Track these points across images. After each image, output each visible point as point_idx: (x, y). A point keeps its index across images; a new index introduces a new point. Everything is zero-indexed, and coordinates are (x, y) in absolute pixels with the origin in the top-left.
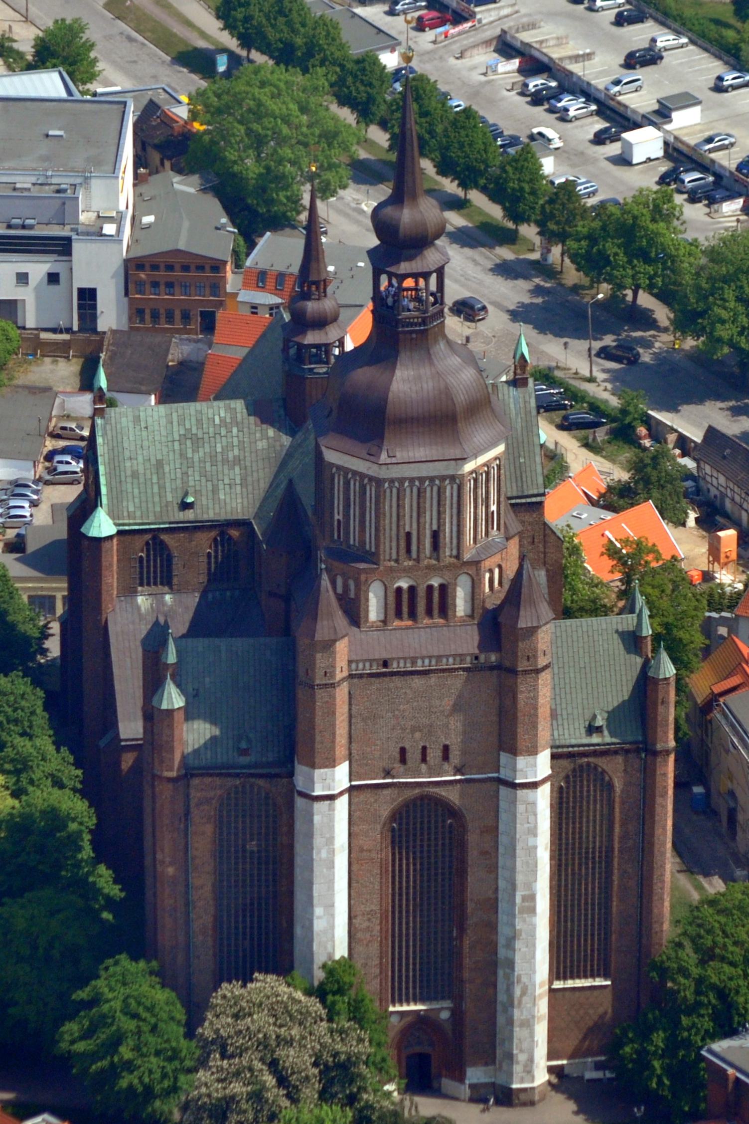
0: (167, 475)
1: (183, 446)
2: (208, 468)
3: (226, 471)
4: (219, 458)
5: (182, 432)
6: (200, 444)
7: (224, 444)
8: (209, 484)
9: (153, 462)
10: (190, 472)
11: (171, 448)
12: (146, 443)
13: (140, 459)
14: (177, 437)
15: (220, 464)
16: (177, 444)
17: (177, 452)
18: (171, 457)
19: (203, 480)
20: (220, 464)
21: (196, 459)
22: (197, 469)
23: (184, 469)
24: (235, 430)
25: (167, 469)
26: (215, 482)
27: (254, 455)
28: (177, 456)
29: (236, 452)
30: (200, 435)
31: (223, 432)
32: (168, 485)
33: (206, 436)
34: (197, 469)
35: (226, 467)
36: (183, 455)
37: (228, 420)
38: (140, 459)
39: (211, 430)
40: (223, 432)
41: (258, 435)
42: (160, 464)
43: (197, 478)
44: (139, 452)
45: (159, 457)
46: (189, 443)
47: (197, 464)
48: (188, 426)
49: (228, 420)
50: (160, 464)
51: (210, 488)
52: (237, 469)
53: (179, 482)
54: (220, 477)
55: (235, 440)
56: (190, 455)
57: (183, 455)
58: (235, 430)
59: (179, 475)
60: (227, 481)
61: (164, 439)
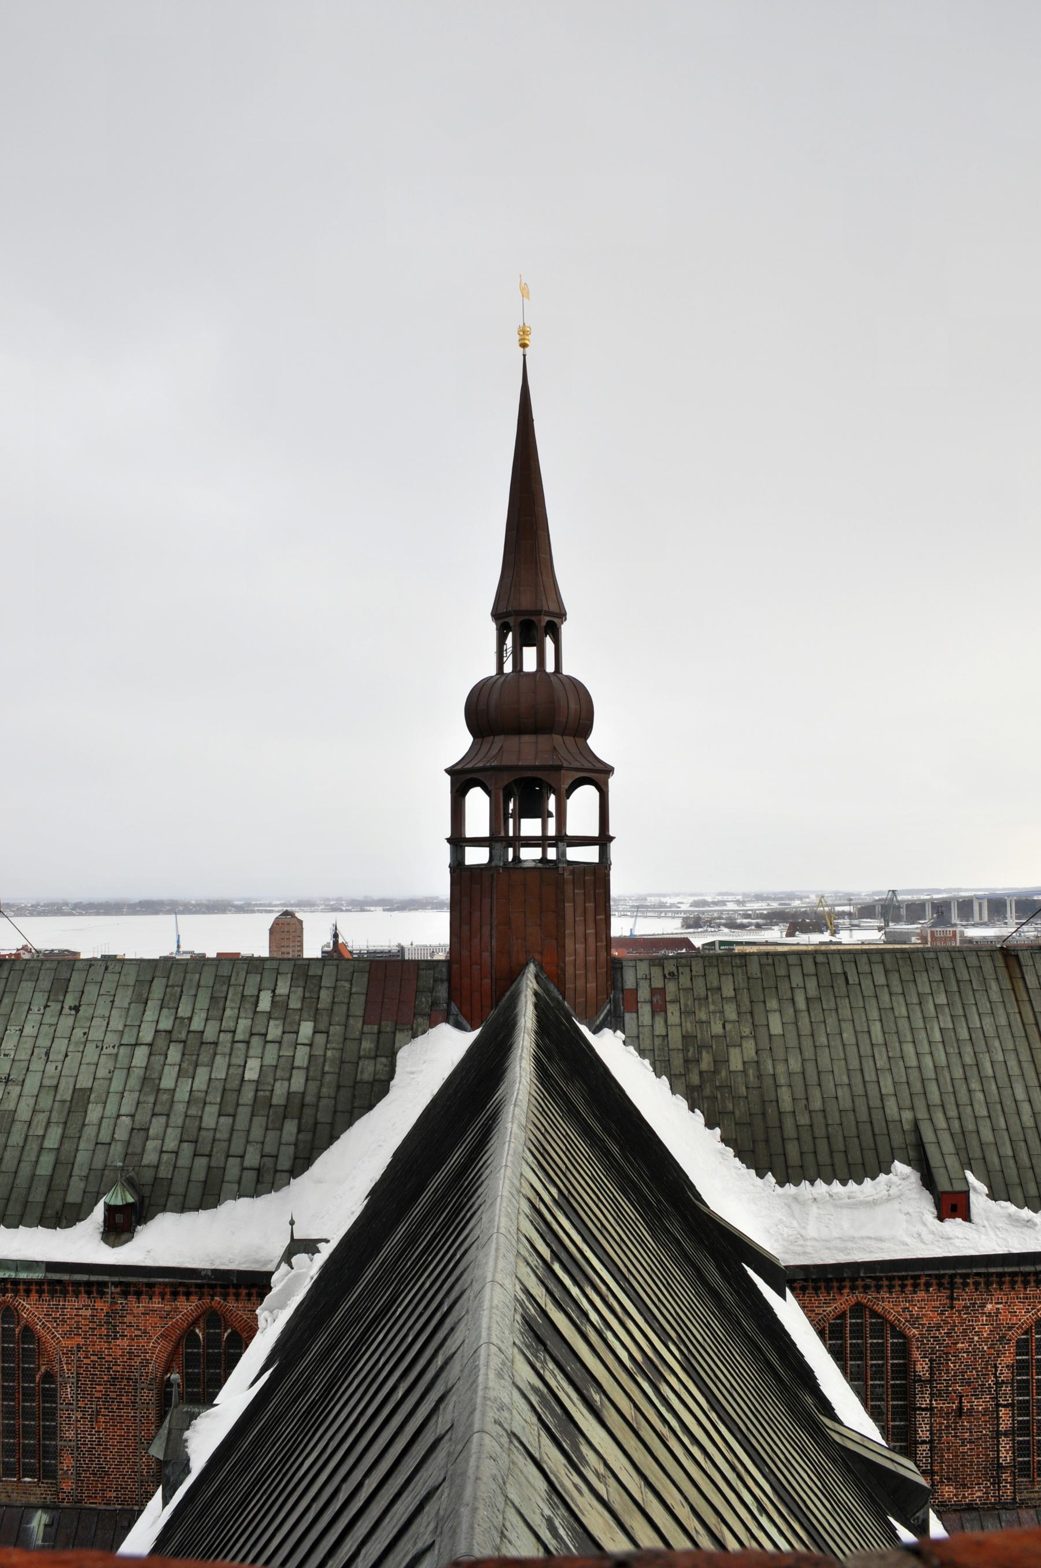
0: (89, 1132)
1: (157, 1059)
2: (209, 1121)
3: (257, 1133)
4: (248, 1095)
5: (165, 1024)
6: (204, 1058)
7: (270, 1059)
8: (201, 1162)
9: (65, 1092)
10: (157, 1125)
11: (122, 1061)
12: (60, 1045)
13: (32, 1083)
14: (147, 1035)
15: (244, 1113)
16: (141, 1053)
17: (137, 1073)
18: (116, 1085)
19: (187, 1149)
20: (244, 1113)
21: (182, 1094)
22: (177, 1119)
23: (142, 1118)
24: (306, 1029)
25: (94, 1114)
26: (218, 1160)
27: (345, 1094)
28: (134, 1082)
29: (298, 1083)
30: (210, 1035)
31: (275, 1030)
32: (82, 1157)
33: (225, 1038)
34: (177, 1119)
35: (259, 1122)
36: (149, 1081)
37: (295, 1004)
38: (32, 1083)
39: (244, 1024)
40: (275, 1030)
41: (367, 1045)
42: (81, 1098)
43: (171, 1144)
44: (37, 1065)
45: (84, 1082)
46: (174, 1054)
47: (180, 1108)
48: (184, 1011)
49: (295, 1004)
50: (81, 1098)
51: (199, 1174)
52: (290, 1128)
53: (117, 1149)
54: (236, 1148)
55: (302, 1053)
56: (167, 1083)
57: (149, 1081)
58: (306, 1029)
59: (122, 1134)
60: (252, 1159)
61: (111, 1039)
